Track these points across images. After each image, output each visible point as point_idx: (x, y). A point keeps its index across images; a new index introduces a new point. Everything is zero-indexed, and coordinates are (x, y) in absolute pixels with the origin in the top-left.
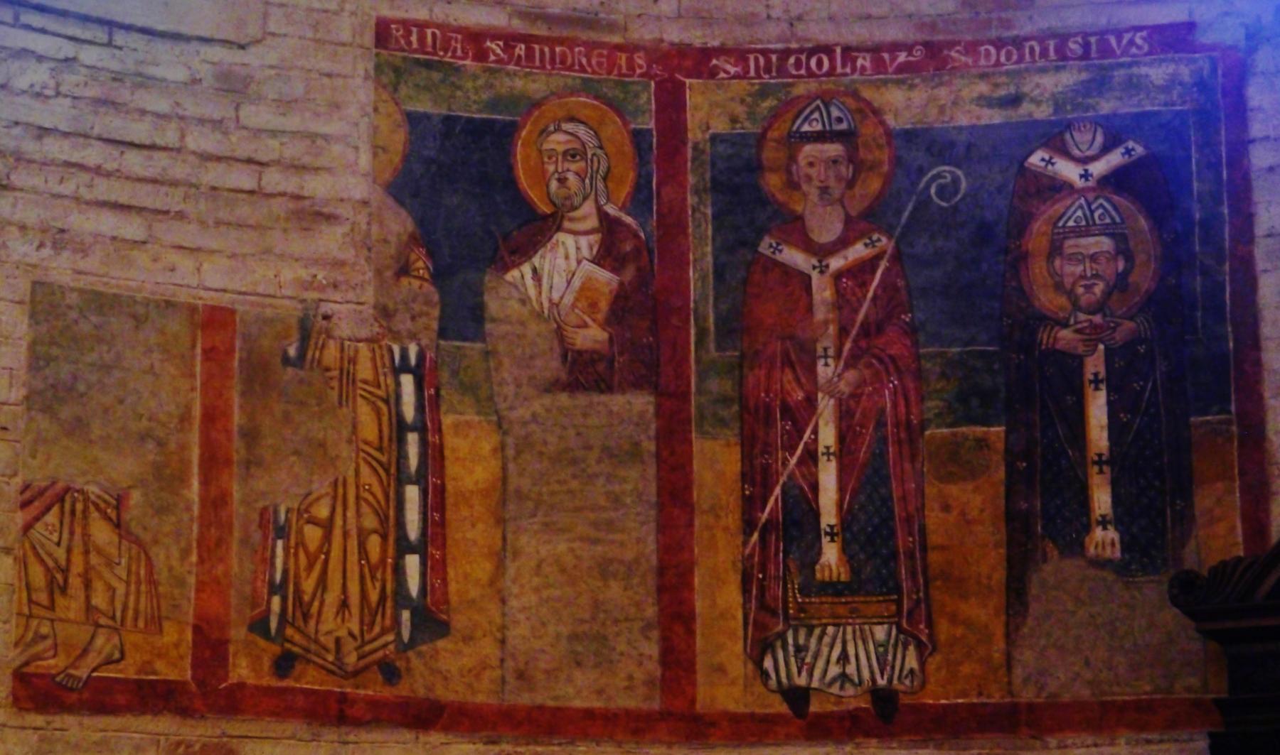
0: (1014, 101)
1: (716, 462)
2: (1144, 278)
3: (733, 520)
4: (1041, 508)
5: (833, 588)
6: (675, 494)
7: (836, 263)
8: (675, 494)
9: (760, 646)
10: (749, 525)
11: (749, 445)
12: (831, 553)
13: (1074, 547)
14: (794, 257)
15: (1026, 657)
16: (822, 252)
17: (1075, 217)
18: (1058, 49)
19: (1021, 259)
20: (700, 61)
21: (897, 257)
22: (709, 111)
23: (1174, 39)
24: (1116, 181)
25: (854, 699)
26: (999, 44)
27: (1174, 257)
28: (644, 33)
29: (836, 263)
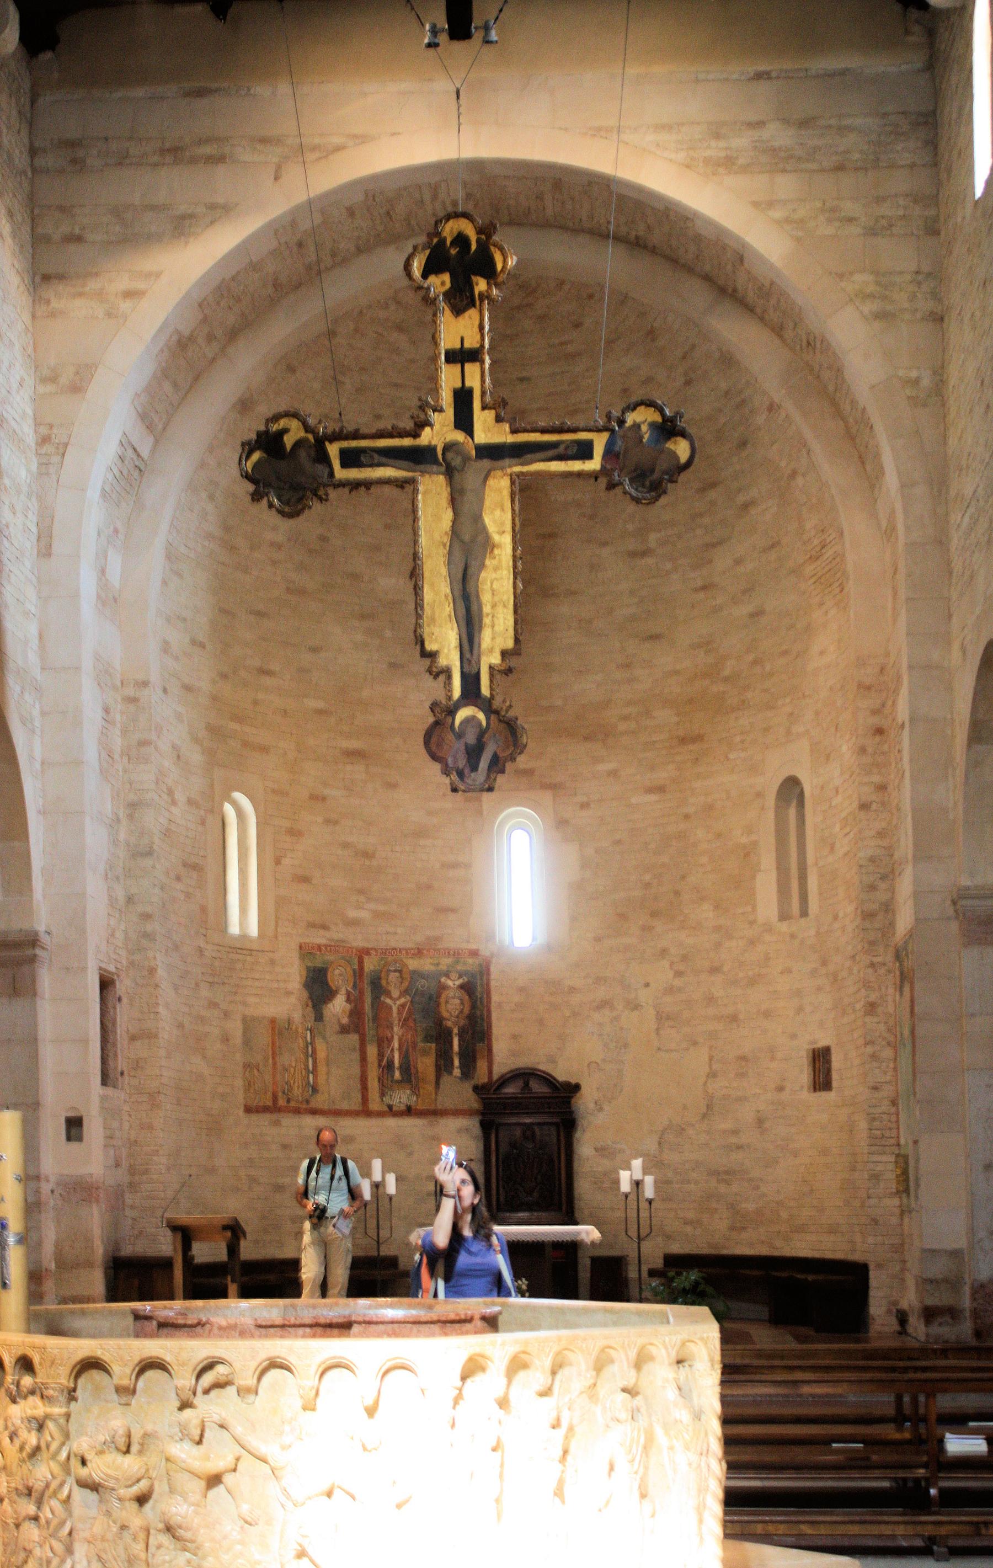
0: (438, 964)
1: (372, 1051)
2: (467, 1011)
3: (376, 1065)
4: (443, 1065)
5: (398, 1082)
6: (363, 1059)
7: (398, 1003)
8: (363, 1059)
9: (383, 1094)
10: (380, 1066)
11: (379, 1046)
12: (397, 1075)
13: (450, 1073)
14: (388, 1001)
15: (440, 1098)
16: (394, 1000)
17: (451, 994)
18: (448, 953)
19: (438, 1005)
20: (367, 952)
21: (412, 1002)
22: (370, 965)
23: (474, 953)
24: (462, 987)
25: (403, 1107)
26: (435, 950)
27: (473, 1007)
28: (355, 944)
29: (398, 1003)
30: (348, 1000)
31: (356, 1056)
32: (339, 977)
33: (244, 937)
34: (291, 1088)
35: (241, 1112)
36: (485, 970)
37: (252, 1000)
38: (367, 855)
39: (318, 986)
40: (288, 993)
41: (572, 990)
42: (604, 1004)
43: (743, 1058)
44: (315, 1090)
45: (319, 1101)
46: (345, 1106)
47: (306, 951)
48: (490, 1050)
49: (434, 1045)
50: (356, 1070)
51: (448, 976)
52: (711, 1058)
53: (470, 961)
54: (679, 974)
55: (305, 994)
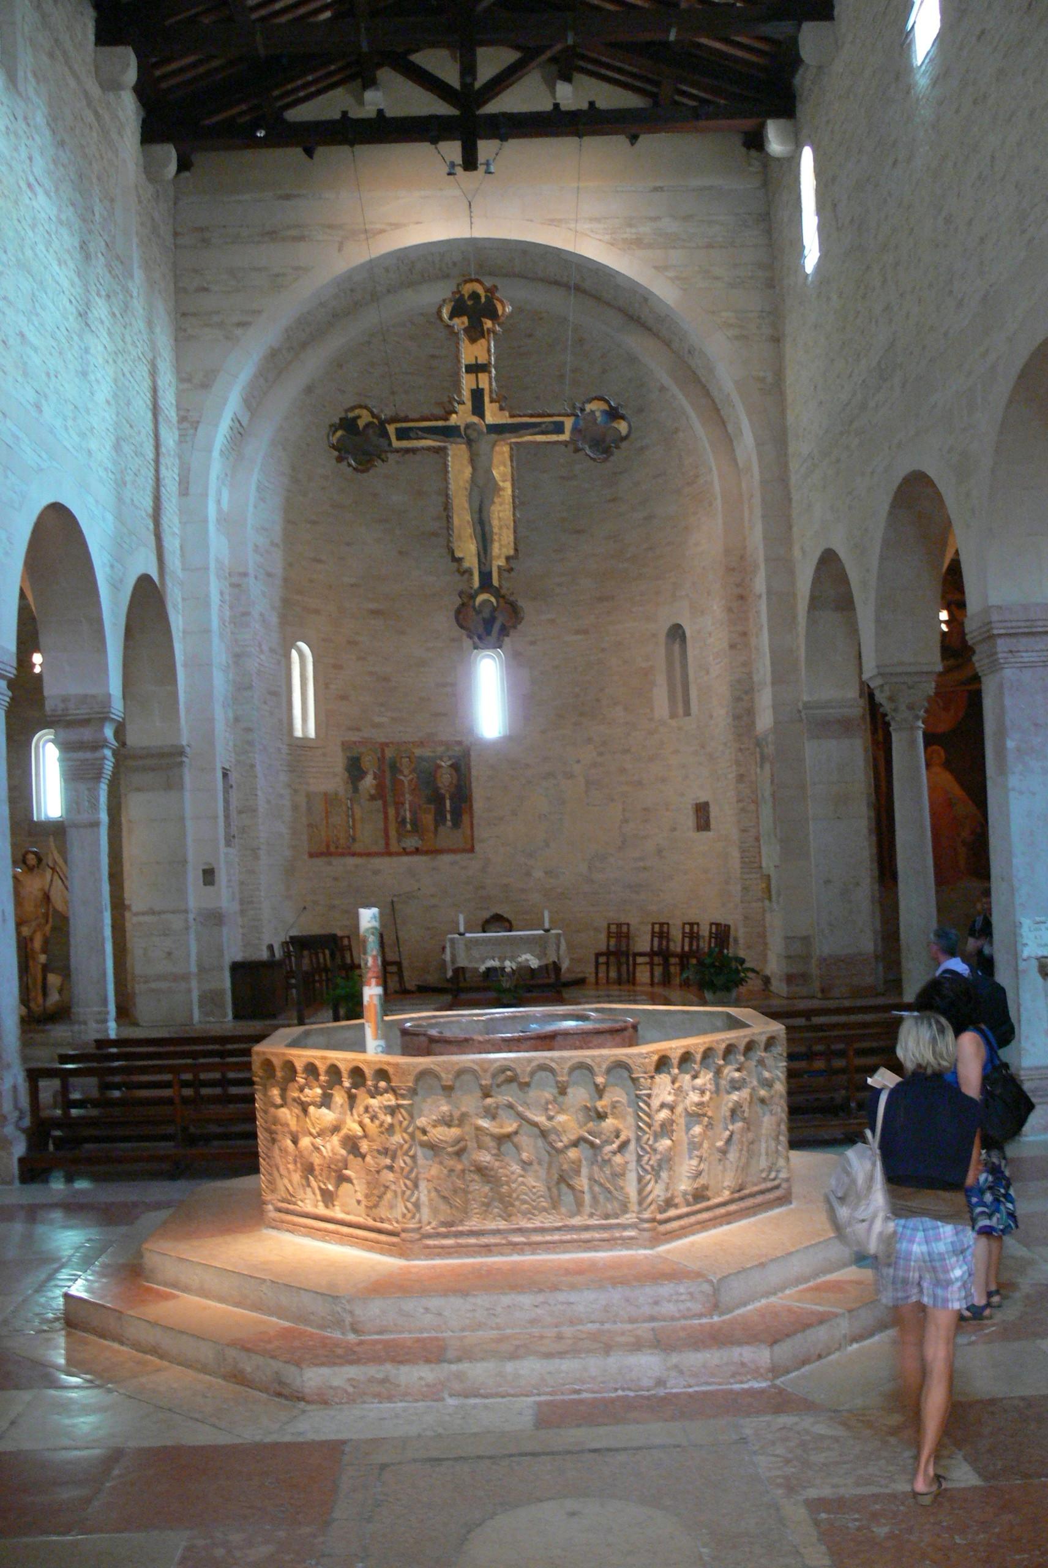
1: (391, 811)
4: (440, 819)
6: (386, 818)
8: (386, 818)
9: (399, 841)
12: (409, 827)
14: (402, 778)
20: (387, 744)
22: (389, 753)
23: (460, 743)
24: (451, 766)
27: (459, 780)
30: (375, 778)
31: (381, 816)
32: (368, 763)
33: (305, 739)
34: (338, 839)
35: (306, 857)
36: (466, 754)
37: (311, 781)
38: (386, 679)
39: (355, 769)
40: (335, 775)
41: (527, 766)
42: (551, 775)
43: (645, 809)
44: (354, 839)
45: (357, 847)
46: (374, 849)
47: (346, 746)
48: (471, 807)
49: (432, 806)
50: (381, 825)
51: (441, 760)
52: (624, 810)
53: (457, 748)
54: (601, 754)
55: (347, 774)
